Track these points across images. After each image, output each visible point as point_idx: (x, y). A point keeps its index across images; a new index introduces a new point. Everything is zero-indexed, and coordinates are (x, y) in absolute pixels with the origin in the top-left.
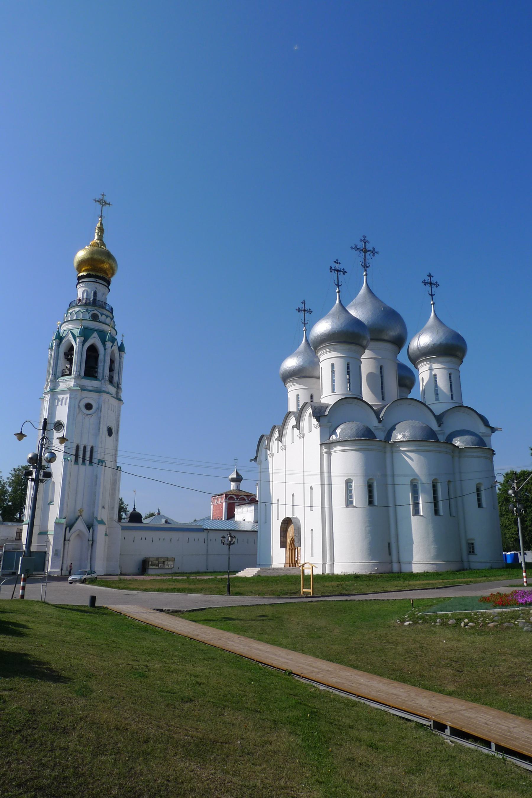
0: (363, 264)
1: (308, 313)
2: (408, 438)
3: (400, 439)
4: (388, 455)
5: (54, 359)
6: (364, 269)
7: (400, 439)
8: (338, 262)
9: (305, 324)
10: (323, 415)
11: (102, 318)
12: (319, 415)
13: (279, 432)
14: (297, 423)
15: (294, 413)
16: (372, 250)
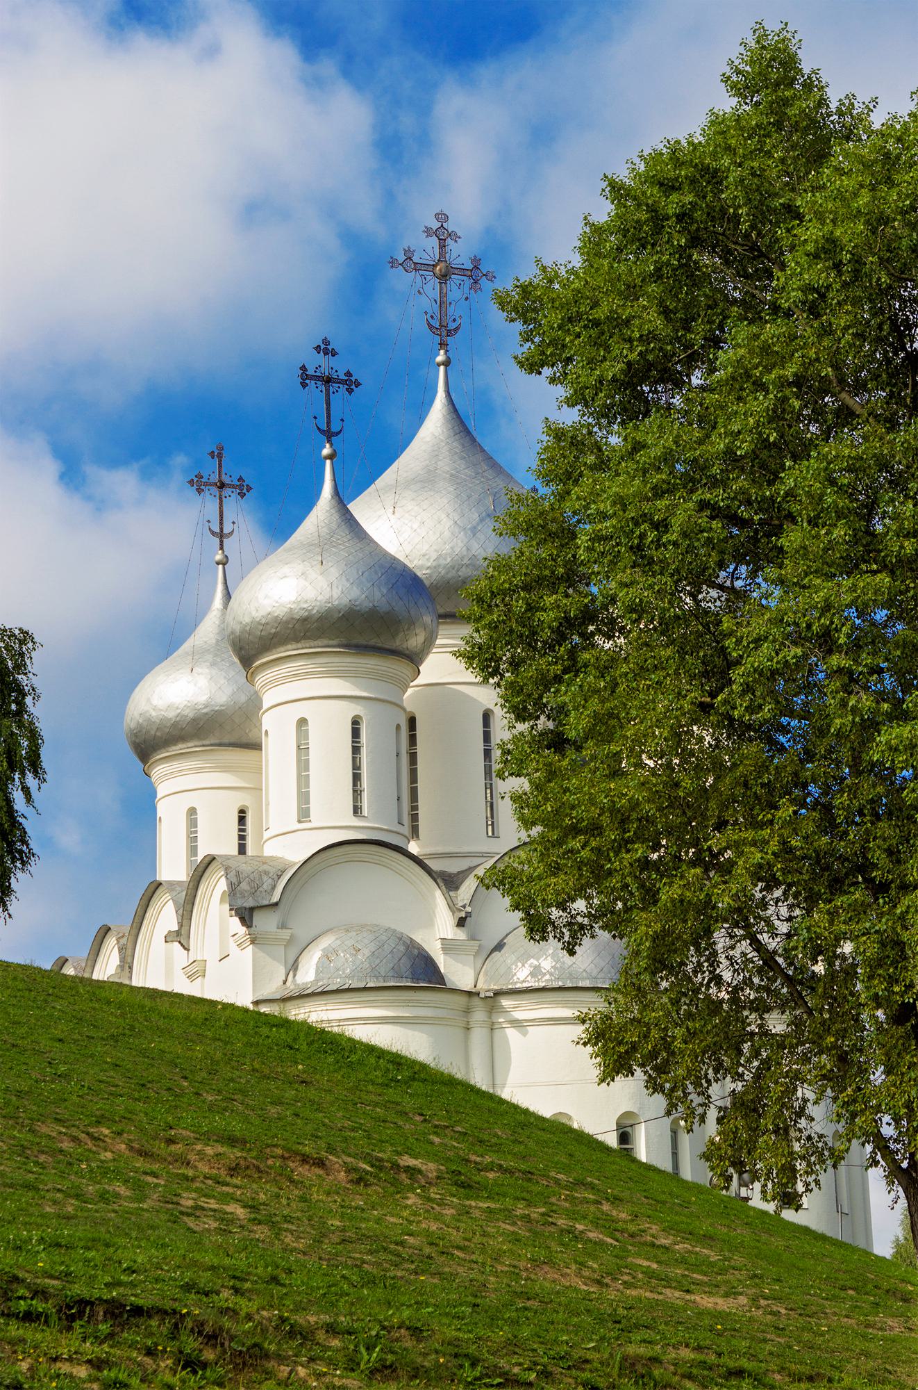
0: (436, 323)
1: (233, 495)
2: (547, 977)
3: (524, 981)
4: (478, 1036)
6: (438, 339)
7: (524, 981)
8: (330, 348)
9: (221, 536)
10: (266, 902)
12: (250, 903)
13: (120, 950)
14: (181, 925)
15: (172, 885)
16: (471, 267)
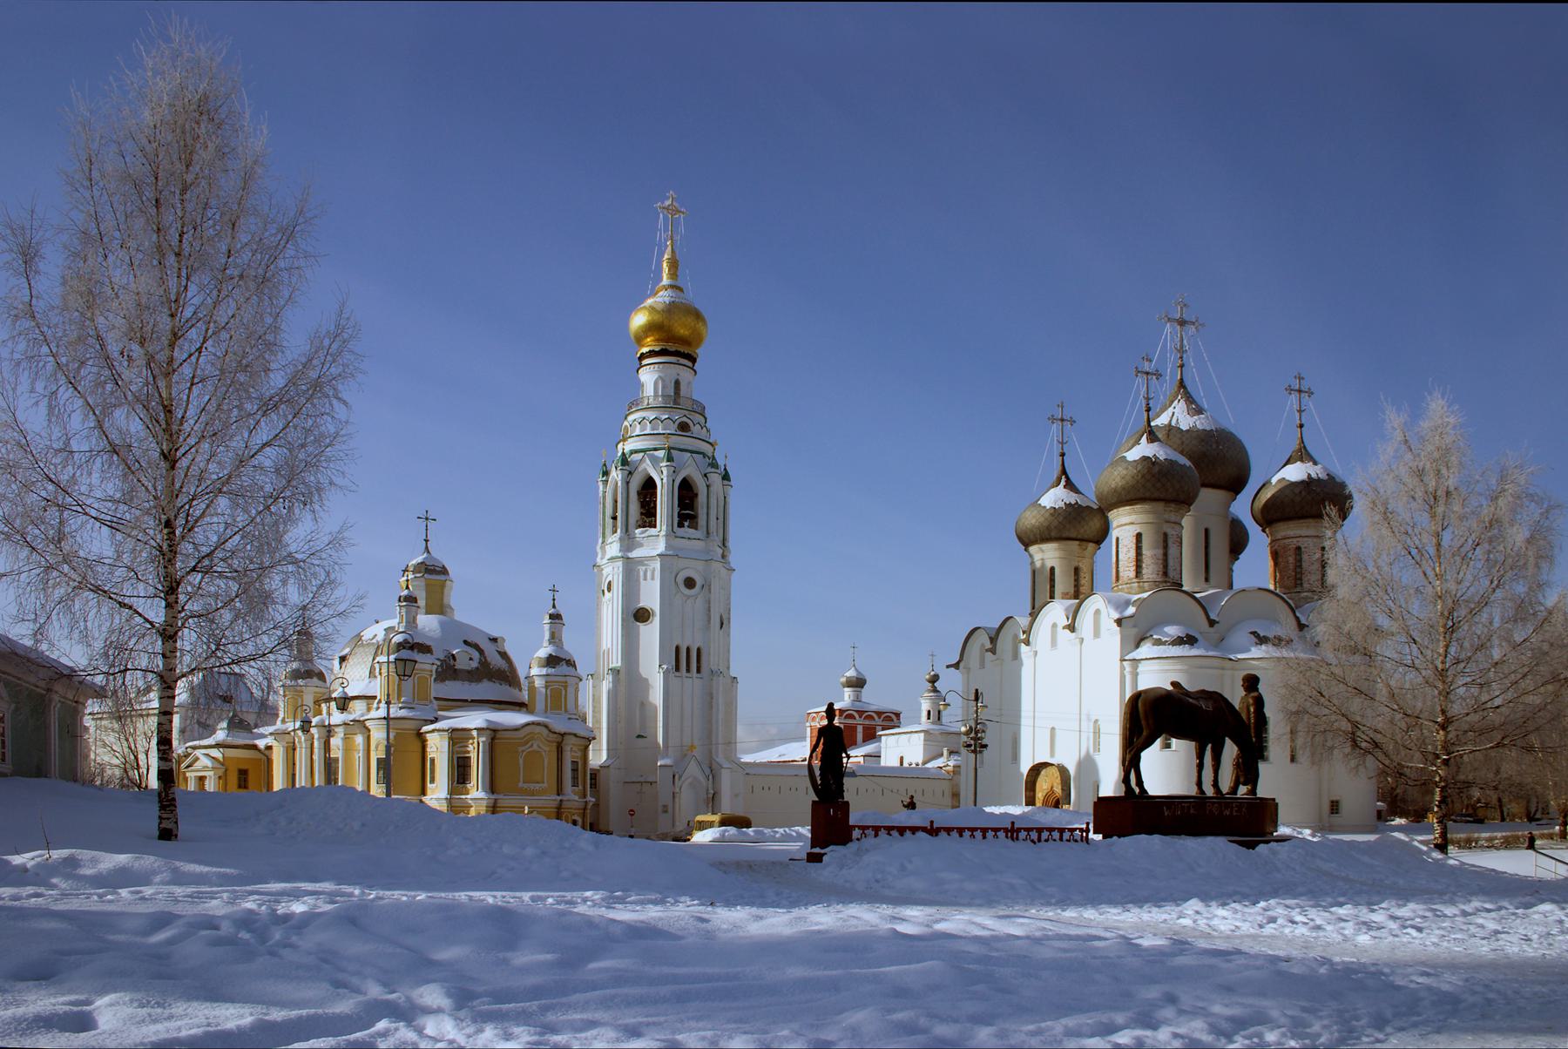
5: (622, 504)
11: (696, 429)
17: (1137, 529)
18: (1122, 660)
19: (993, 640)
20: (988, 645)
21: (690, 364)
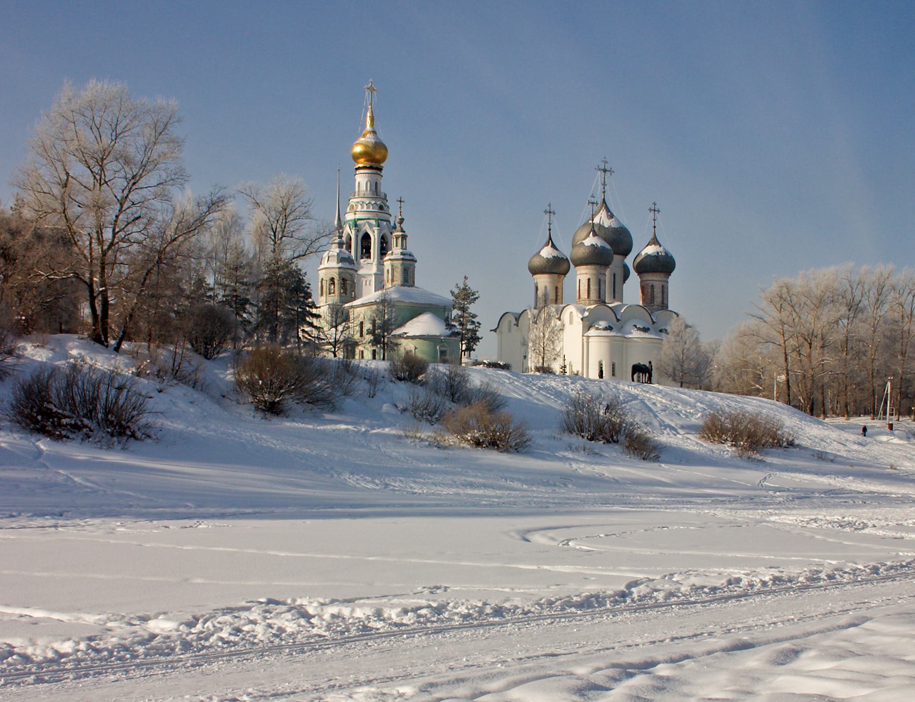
17: (588, 276)
18: (583, 336)
19: (517, 319)
20: (514, 322)
21: (379, 172)
